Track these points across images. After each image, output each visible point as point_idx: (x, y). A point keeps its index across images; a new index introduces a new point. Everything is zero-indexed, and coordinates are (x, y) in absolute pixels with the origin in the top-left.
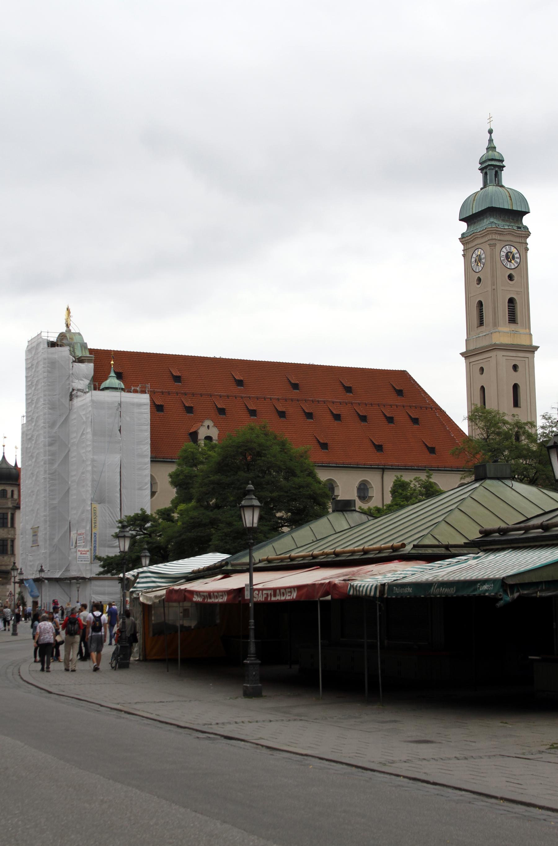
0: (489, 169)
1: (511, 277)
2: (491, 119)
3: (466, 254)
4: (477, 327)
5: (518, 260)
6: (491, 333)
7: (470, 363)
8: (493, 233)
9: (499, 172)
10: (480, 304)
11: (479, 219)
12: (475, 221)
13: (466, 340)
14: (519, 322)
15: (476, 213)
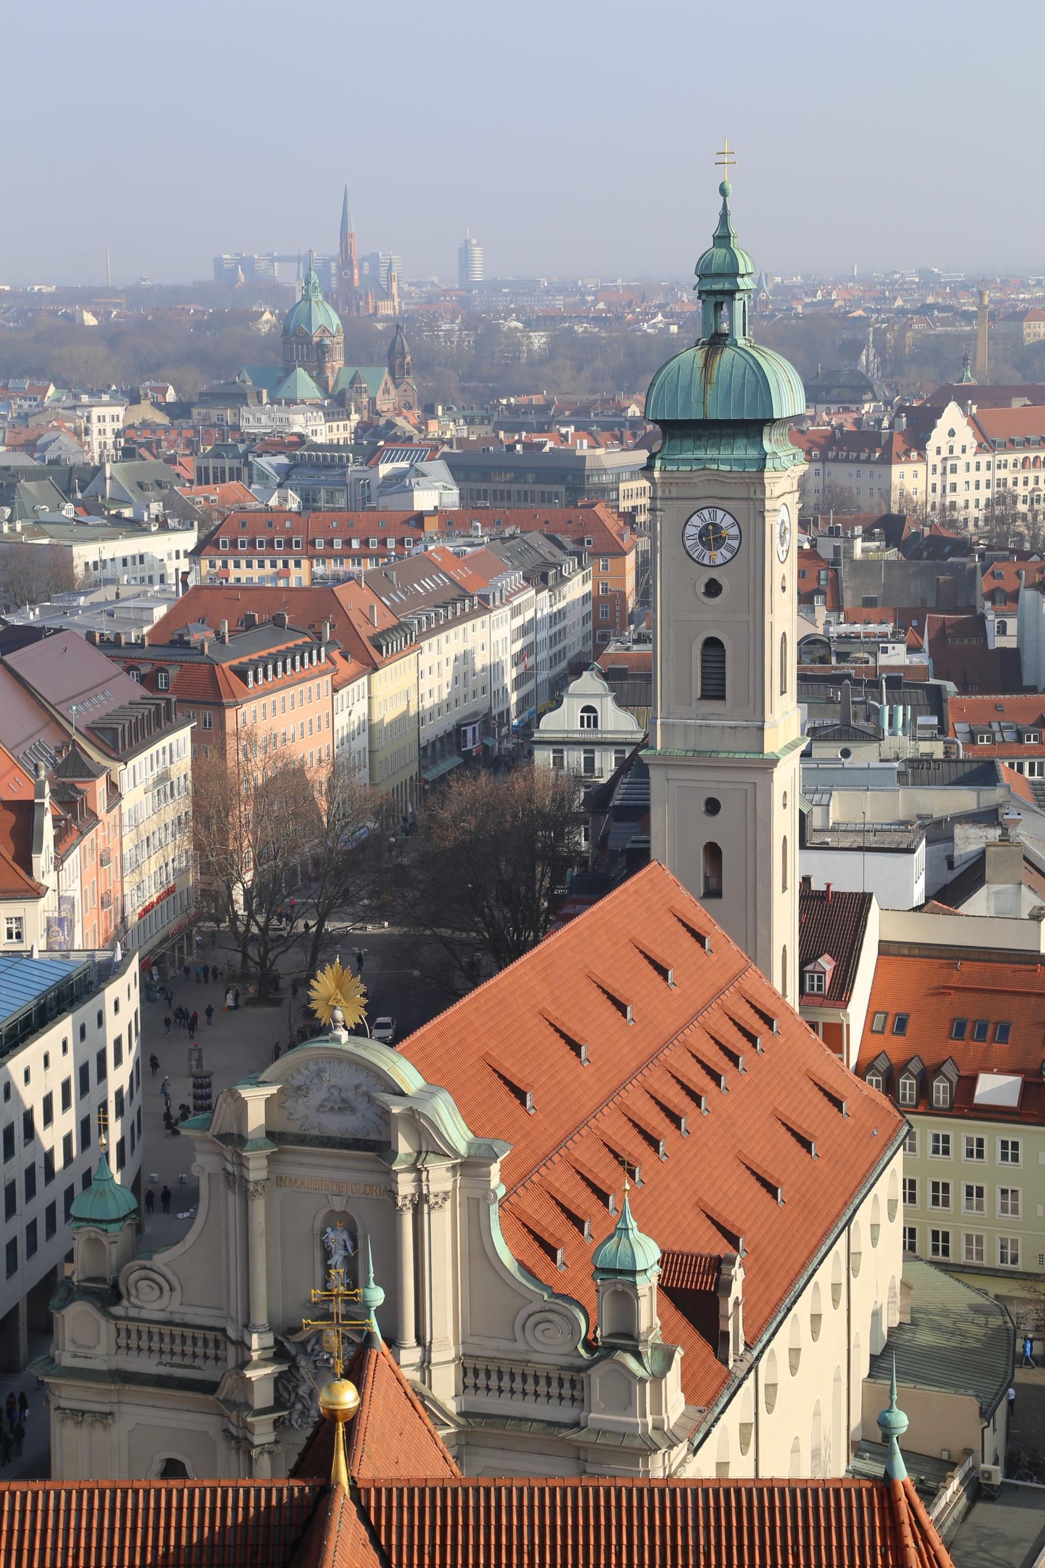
10: (713, 644)
11: (718, 431)
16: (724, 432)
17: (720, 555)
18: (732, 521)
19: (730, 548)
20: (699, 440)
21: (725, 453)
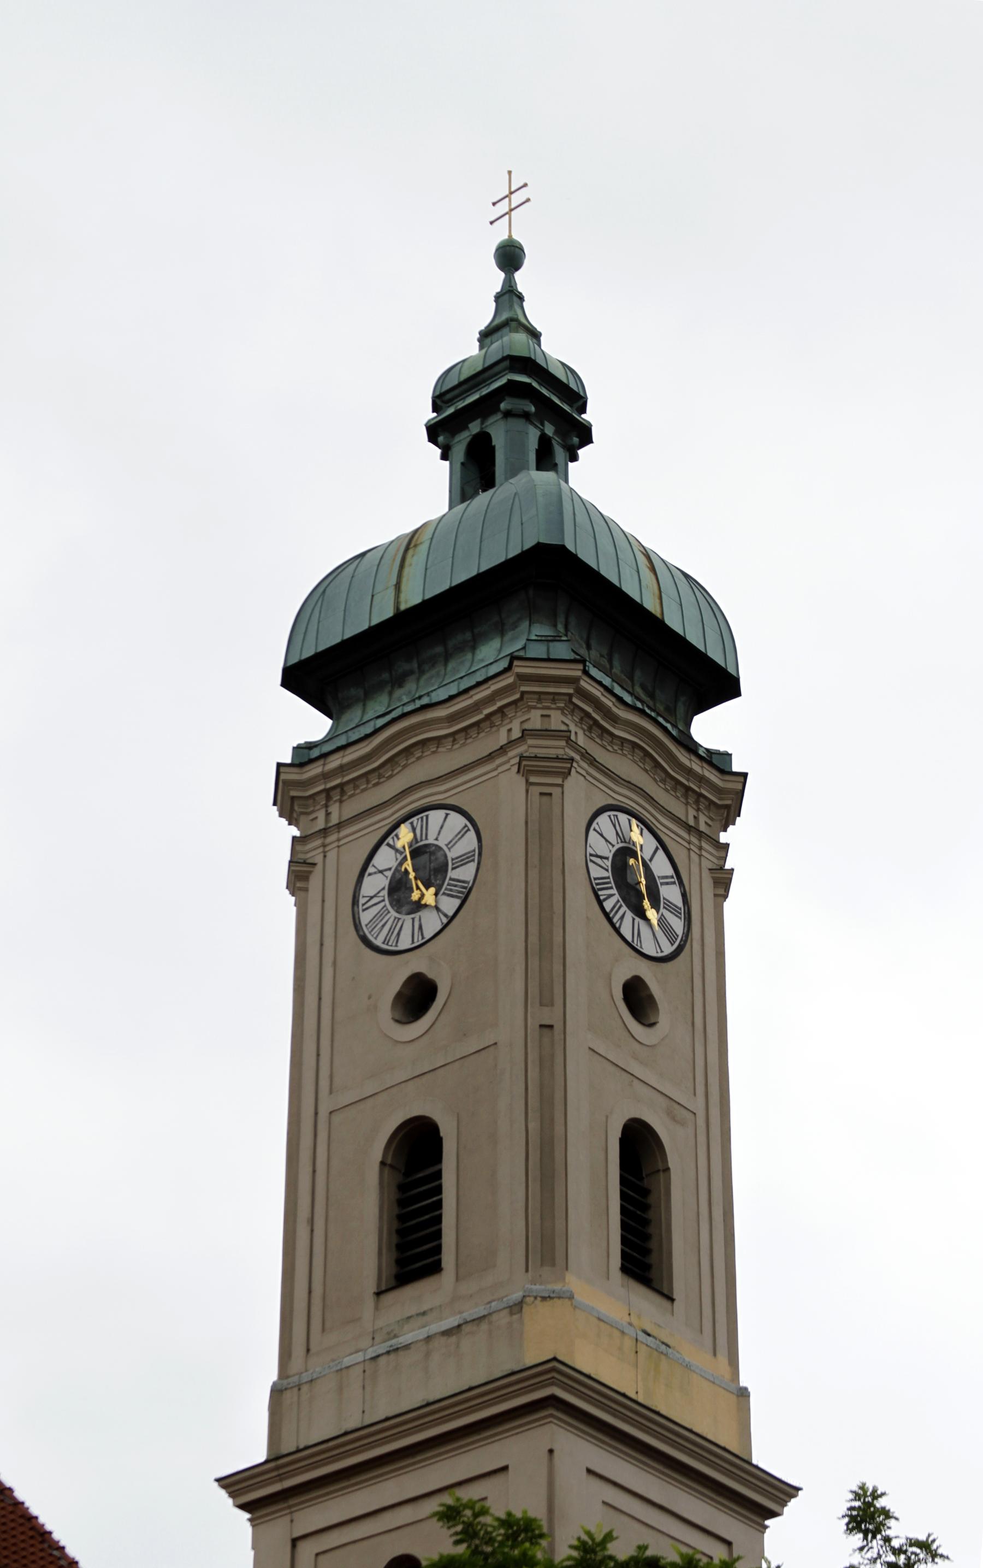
0: (508, 414)
2: (517, 199)
3: (319, 859)
4: (378, 1294)
5: (678, 925)
6: (517, 1307)
7: (294, 1542)
8: (555, 697)
9: (560, 454)
11: (439, 649)
12: (403, 666)
13: (277, 1392)
14: (679, 1288)
15: (425, 603)
16: (451, 643)
20: (400, 686)
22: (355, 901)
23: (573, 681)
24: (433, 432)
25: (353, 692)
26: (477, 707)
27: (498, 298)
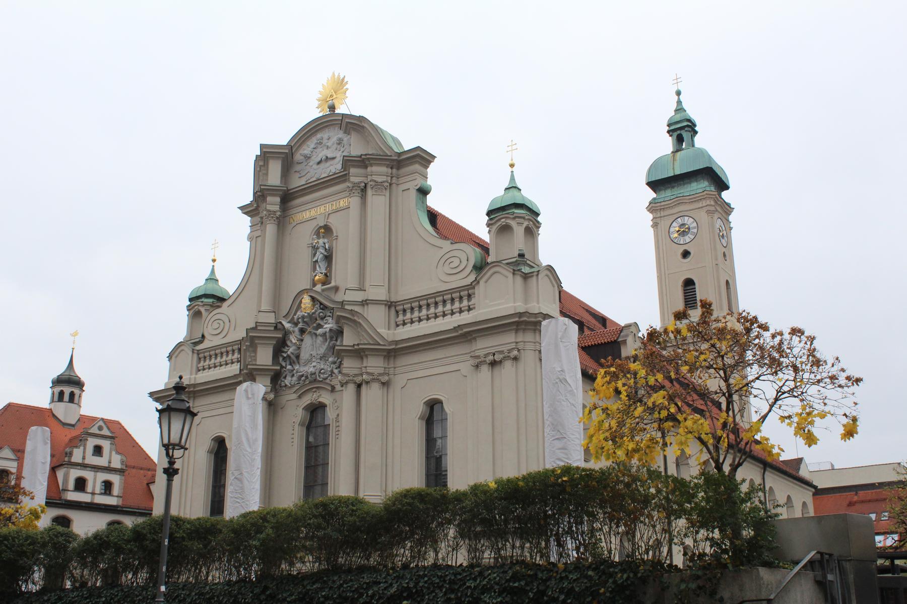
0: (686, 131)
1: (724, 255)
2: (679, 80)
3: (659, 222)
5: (726, 239)
12: (674, 185)
17: (687, 239)
18: (693, 220)
19: (693, 233)
21: (686, 190)
22: (669, 232)
23: (715, 195)
24: (668, 132)
25: (662, 188)
26: (695, 198)
27: (677, 102)
